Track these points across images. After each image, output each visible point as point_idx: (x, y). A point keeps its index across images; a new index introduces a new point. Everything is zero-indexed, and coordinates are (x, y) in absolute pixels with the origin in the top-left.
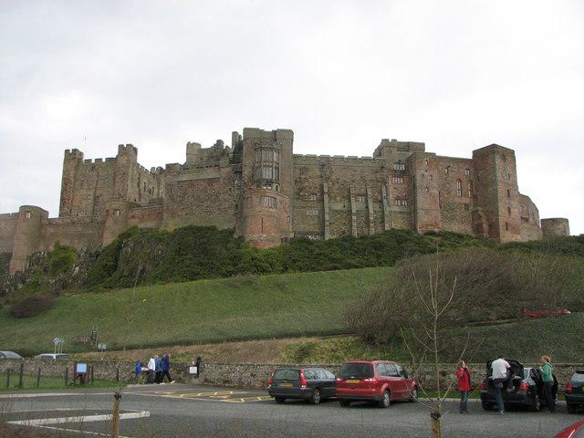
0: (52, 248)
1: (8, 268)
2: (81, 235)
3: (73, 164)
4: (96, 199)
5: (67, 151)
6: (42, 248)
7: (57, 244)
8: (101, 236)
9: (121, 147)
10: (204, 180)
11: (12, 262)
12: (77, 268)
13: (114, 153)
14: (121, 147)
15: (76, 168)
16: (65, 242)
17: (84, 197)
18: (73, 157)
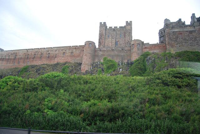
0: (102, 61)
1: (80, 69)
2: (118, 56)
3: (104, 28)
4: (116, 43)
5: (101, 23)
6: (96, 60)
7: (105, 59)
8: (130, 56)
9: (127, 22)
10: (187, 31)
11: (82, 66)
12: (121, 70)
13: (124, 24)
14: (127, 22)
15: (106, 30)
16: (109, 58)
17: (110, 42)
18: (103, 26)
